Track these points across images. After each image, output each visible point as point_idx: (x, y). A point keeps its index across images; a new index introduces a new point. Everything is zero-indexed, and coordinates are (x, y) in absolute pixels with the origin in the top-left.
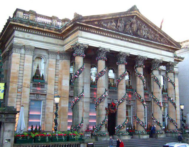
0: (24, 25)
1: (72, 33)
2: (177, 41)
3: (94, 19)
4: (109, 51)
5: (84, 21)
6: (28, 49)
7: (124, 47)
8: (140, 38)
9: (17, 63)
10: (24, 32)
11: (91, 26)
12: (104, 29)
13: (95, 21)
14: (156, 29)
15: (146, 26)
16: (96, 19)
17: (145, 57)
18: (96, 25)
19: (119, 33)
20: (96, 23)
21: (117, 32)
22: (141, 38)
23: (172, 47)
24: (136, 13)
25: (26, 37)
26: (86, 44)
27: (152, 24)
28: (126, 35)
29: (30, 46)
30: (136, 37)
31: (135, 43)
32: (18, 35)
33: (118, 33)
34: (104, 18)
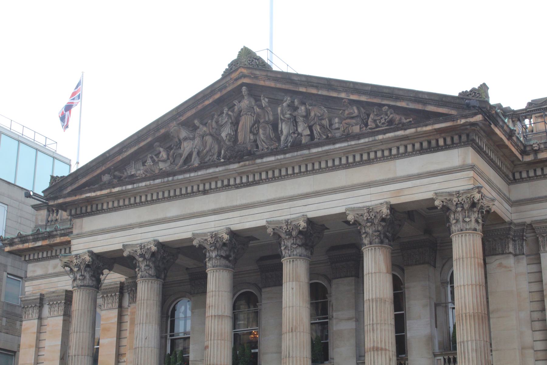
0: (30, 245)
1: (489, 157)
2: (455, 92)
3: (99, 171)
4: (154, 248)
5: (69, 189)
6: (55, 300)
7: (215, 212)
8: (259, 161)
9: (30, 346)
10: (43, 259)
11: (88, 195)
12: (124, 188)
13: (103, 173)
14: (335, 90)
15: (296, 103)
16: (104, 168)
17: (297, 219)
18: (111, 185)
19: (176, 178)
20: (106, 178)
21: (166, 179)
22: (262, 156)
23: (437, 126)
24: (245, 76)
25: (51, 271)
26: (85, 253)
27: (310, 81)
28: (211, 170)
29: (53, 292)
30: (84, 196)
31: (115, 211)
32: (34, 271)
33: (170, 179)
34: (125, 152)
